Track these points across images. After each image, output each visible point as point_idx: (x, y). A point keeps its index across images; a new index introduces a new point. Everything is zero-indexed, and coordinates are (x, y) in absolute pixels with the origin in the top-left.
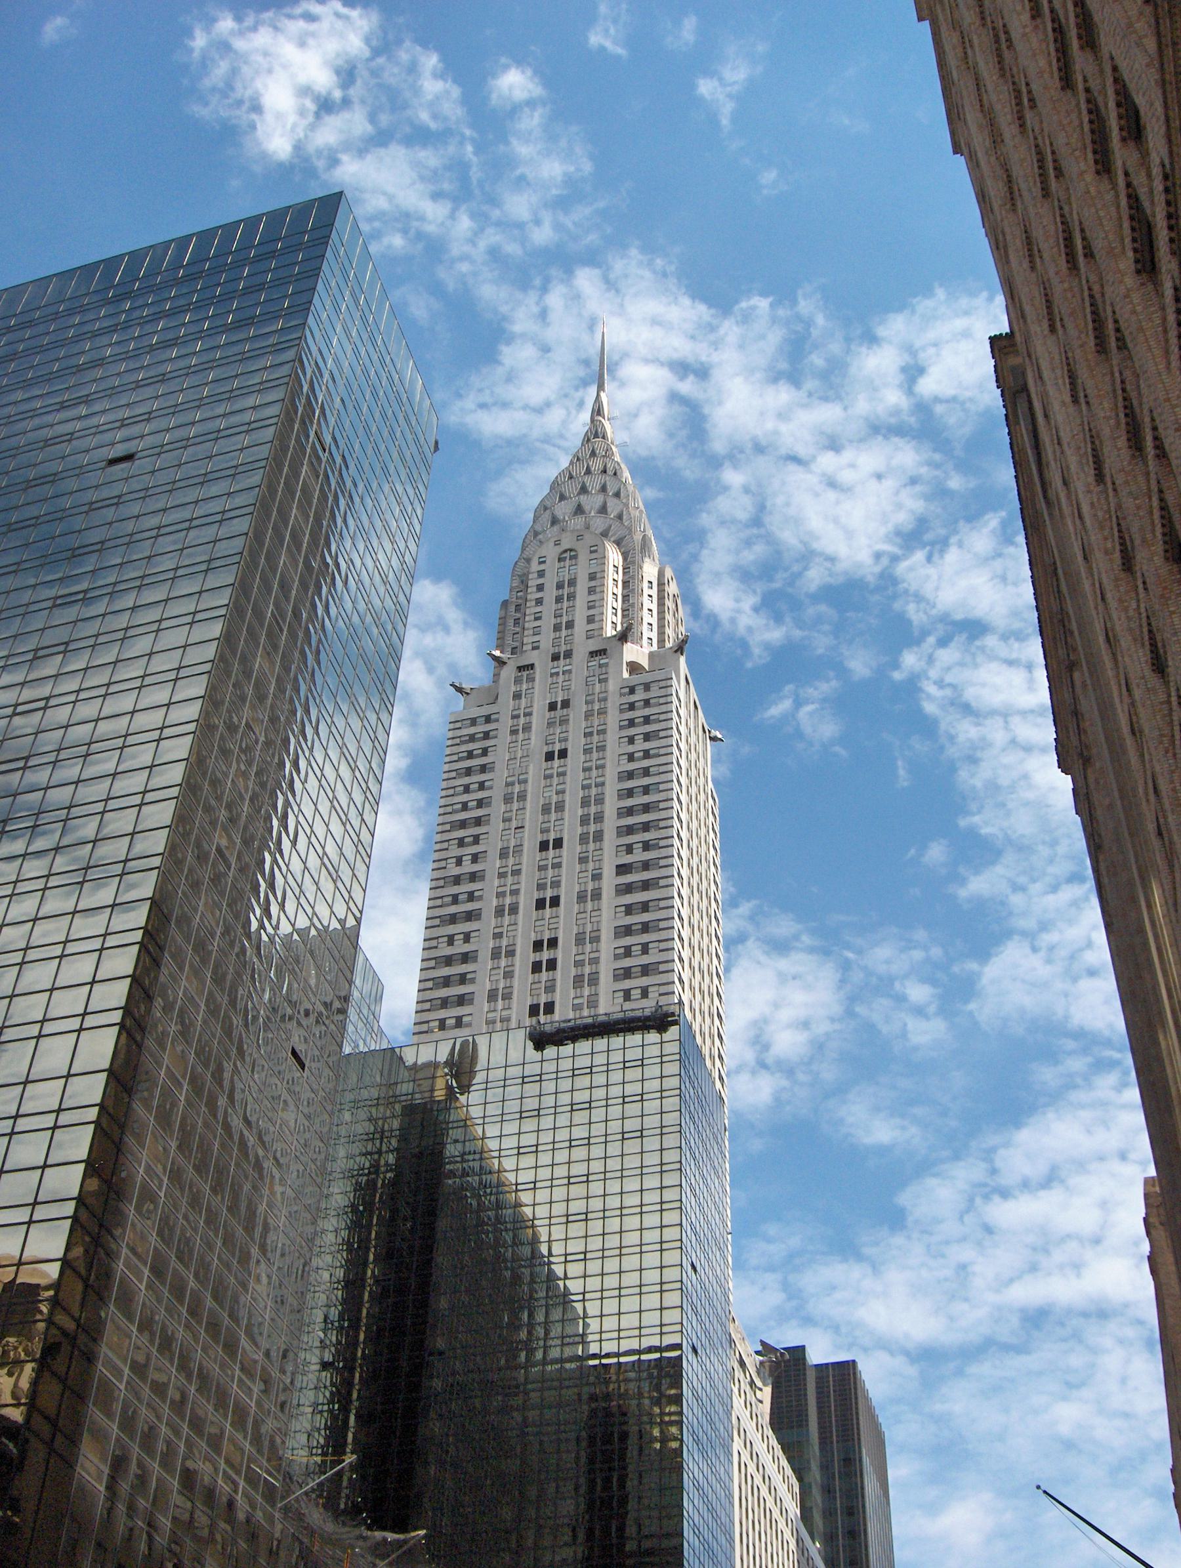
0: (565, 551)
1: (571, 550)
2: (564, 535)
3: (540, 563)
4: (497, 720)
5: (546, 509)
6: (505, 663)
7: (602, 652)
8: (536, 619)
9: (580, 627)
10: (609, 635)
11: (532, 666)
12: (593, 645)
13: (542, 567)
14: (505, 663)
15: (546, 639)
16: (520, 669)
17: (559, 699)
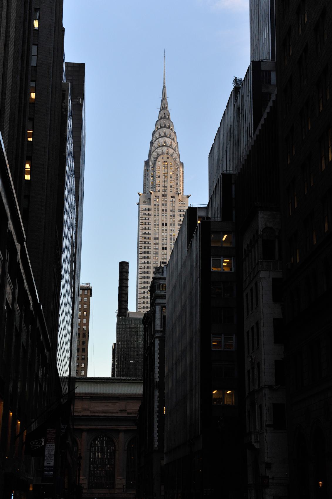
9: (169, 189)
15: (161, 189)
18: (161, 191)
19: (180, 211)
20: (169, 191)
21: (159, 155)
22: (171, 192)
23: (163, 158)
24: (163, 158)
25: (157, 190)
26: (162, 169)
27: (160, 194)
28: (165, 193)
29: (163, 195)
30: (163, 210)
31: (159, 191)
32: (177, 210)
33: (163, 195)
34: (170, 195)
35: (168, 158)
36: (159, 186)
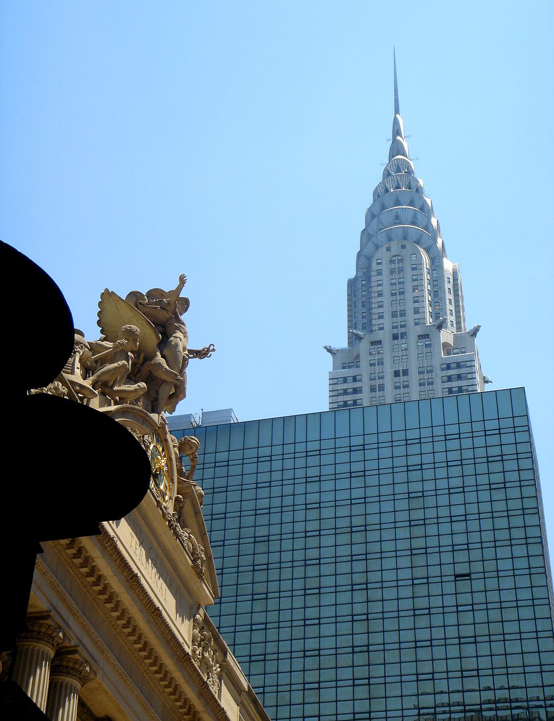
0: (395, 256)
1: (398, 256)
2: (392, 243)
3: (378, 264)
4: (361, 381)
5: (374, 216)
6: (362, 338)
7: (425, 336)
8: (380, 307)
9: (411, 317)
10: (428, 324)
11: (380, 342)
12: (419, 330)
13: (379, 267)
14: (362, 338)
15: (387, 322)
16: (373, 343)
17: (401, 369)
18: (387, 327)
19: (449, 367)
20: (411, 324)
21: (377, 247)
22: (416, 324)
23: (388, 249)
24: (388, 249)
25: (375, 328)
26: (385, 277)
27: (384, 336)
28: (400, 331)
29: (395, 337)
30: (397, 374)
31: (381, 329)
32: (437, 364)
33: (395, 337)
34: (414, 332)
35: (403, 247)
36: (381, 317)
